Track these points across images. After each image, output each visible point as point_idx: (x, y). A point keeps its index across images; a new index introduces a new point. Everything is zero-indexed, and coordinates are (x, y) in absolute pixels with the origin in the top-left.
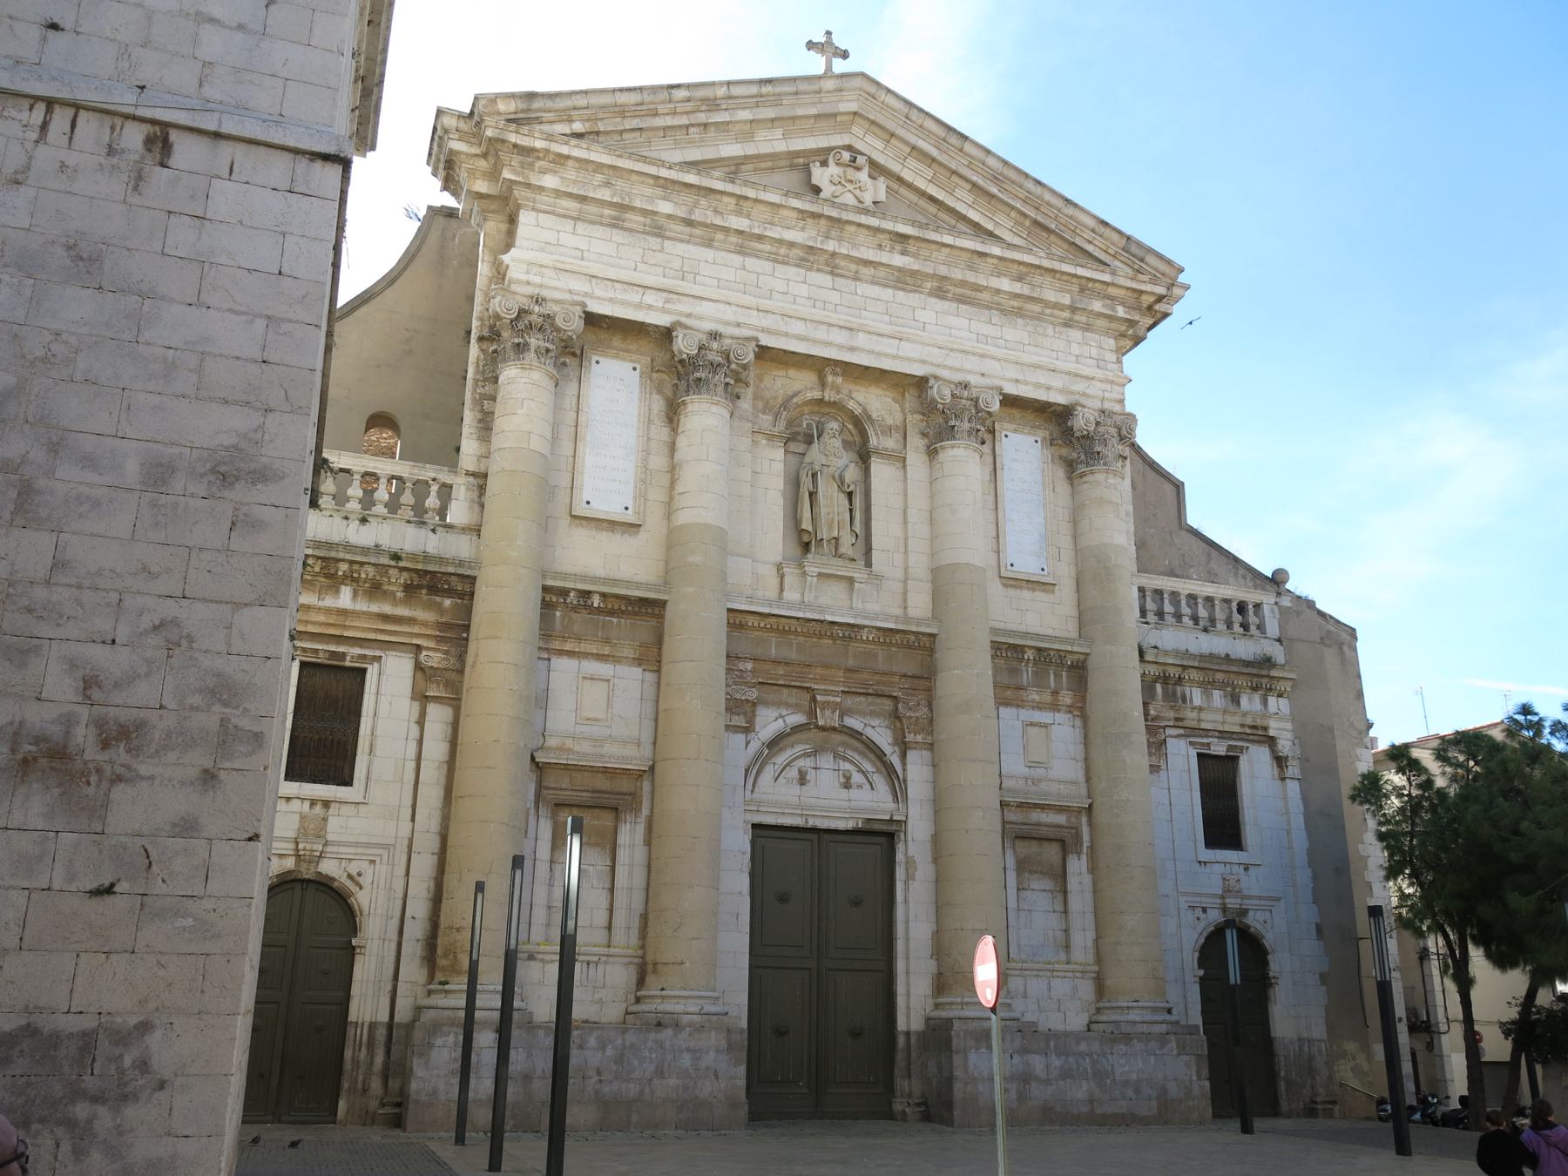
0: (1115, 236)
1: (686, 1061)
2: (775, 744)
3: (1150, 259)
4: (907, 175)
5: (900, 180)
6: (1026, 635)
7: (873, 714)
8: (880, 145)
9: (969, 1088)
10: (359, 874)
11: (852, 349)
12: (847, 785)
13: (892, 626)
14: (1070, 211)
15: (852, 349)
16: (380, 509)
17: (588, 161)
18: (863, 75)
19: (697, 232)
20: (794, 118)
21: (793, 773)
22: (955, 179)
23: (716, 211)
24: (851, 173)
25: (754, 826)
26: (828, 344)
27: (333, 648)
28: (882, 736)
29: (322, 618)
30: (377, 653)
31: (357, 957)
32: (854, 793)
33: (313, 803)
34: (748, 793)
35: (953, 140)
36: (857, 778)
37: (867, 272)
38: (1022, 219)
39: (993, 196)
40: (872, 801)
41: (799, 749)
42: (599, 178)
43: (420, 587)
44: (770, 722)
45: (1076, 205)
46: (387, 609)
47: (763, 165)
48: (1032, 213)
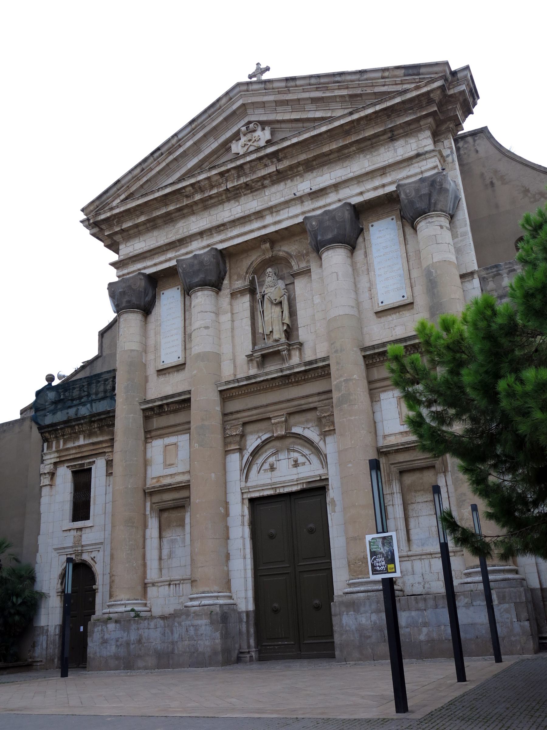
1: (192, 631)
2: (255, 453)
3: (422, 70)
4: (279, 117)
7: (307, 421)
8: (261, 111)
9: (344, 637)
10: (94, 557)
11: (264, 227)
12: (296, 464)
13: (303, 368)
14: (366, 76)
15: (264, 227)
19: (185, 211)
20: (215, 128)
21: (267, 466)
23: (187, 197)
24: (249, 136)
25: (252, 501)
26: (252, 231)
27: (80, 462)
28: (312, 434)
29: (74, 451)
30: (94, 459)
31: (97, 594)
32: (300, 469)
33: (77, 529)
34: (243, 484)
35: (291, 83)
36: (301, 460)
37: (266, 182)
40: (310, 470)
41: (269, 453)
42: (138, 213)
43: (102, 426)
44: (252, 442)
46: (95, 440)
47: (212, 159)
48: (344, 92)
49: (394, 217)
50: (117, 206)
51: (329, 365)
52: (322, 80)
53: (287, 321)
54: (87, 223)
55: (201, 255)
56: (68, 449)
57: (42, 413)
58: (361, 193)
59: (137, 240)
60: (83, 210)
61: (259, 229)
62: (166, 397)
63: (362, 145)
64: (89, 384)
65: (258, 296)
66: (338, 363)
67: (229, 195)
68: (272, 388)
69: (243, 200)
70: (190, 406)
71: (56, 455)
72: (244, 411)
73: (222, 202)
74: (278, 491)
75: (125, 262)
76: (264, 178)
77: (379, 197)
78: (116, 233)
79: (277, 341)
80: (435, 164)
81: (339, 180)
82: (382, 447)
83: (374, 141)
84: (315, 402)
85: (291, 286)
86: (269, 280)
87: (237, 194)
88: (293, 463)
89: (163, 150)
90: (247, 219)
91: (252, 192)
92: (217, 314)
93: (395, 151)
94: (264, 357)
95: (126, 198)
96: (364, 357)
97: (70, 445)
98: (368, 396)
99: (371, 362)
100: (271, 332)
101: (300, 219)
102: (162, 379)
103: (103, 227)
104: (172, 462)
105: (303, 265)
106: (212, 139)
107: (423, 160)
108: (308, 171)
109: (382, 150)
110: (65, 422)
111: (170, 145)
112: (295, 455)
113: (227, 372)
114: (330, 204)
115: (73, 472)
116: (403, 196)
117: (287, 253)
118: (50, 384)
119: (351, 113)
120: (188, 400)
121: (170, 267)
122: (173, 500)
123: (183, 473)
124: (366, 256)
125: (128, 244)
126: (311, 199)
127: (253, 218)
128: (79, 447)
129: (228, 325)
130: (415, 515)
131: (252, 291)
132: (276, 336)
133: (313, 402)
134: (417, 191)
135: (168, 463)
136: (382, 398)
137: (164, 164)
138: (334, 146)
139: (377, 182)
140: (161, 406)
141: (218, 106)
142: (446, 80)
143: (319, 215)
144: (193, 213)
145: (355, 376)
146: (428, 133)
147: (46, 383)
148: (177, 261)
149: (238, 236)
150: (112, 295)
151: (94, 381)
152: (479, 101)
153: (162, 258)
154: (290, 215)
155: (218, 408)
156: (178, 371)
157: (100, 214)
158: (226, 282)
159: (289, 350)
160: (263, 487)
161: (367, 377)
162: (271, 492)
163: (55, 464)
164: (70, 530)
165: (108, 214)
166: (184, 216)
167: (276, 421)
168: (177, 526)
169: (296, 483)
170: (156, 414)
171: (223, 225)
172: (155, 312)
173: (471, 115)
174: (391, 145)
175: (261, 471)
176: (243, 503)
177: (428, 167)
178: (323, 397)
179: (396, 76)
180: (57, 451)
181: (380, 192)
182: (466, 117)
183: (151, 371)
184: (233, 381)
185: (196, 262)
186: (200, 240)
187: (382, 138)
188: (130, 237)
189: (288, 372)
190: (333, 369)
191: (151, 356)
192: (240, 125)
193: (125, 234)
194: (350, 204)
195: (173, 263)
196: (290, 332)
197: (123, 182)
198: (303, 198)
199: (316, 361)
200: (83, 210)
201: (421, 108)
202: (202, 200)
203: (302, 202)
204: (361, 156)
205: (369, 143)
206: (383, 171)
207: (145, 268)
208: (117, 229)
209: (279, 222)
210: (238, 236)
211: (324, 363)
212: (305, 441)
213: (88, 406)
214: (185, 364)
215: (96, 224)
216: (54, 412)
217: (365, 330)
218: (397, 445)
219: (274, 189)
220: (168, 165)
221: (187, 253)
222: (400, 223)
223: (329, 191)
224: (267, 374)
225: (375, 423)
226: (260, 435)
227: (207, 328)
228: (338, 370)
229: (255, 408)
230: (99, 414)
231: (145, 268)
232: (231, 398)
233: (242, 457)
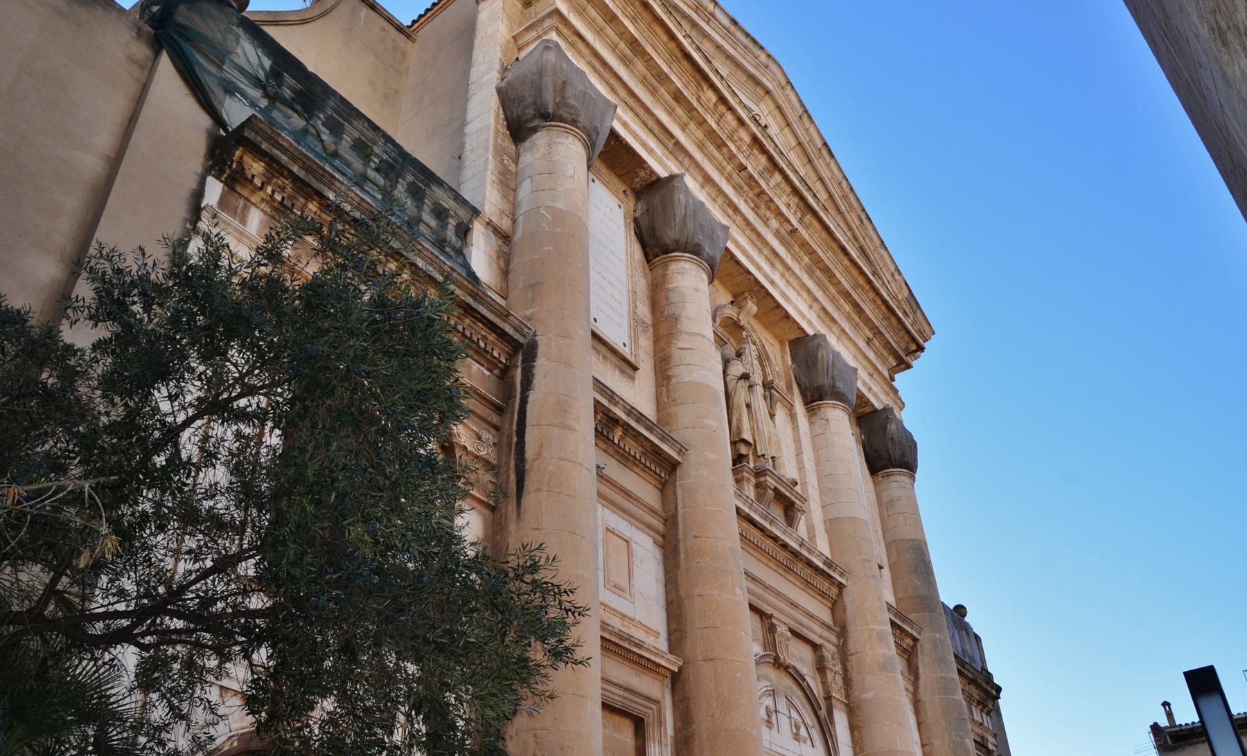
14: (883, 252)
67: (735, 176)
76: (779, 214)
87: (741, 188)
121: (645, 162)
122: (627, 689)
188: (581, 14)
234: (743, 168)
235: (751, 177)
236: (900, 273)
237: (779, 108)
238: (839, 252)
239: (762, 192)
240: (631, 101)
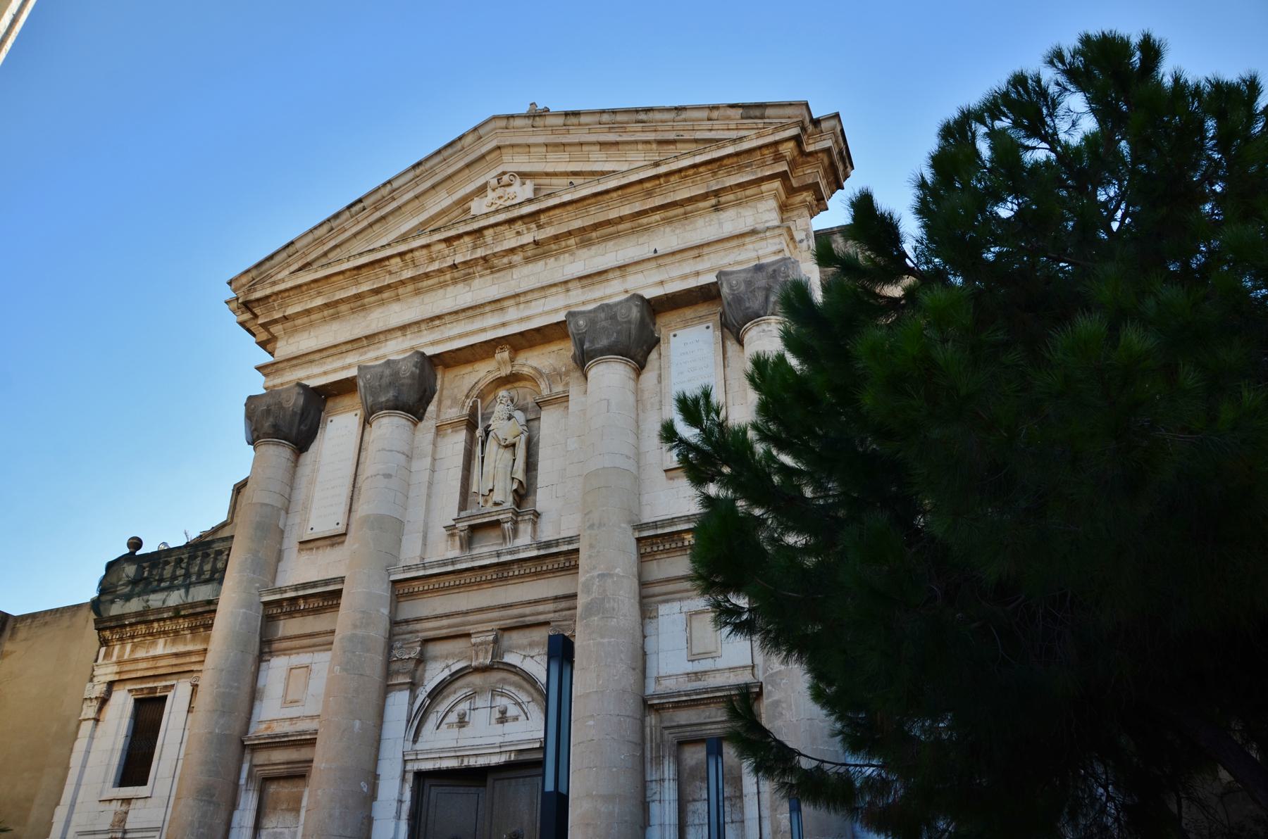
0: (731, 112)
2: (437, 693)
4: (550, 168)
5: (547, 174)
6: (672, 521)
7: (532, 645)
8: (524, 158)
11: (504, 325)
12: (503, 718)
13: (534, 553)
14: (684, 115)
15: (504, 325)
16: (194, 579)
17: (300, 286)
18: (494, 118)
19: (385, 295)
20: (449, 177)
21: (453, 718)
22: (585, 148)
23: (390, 273)
24: (500, 192)
25: (419, 775)
26: (484, 330)
33: (123, 800)
34: (409, 745)
35: (573, 120)
37: (517, 258)
38: (649, 146)
39: (617, 143)
41: (460, 694)
42: (313, 292)
43: (197, 627)
44: (435, 674)
45: (683, 109)
46: (181, 648)
49: (710, 324)
50: (283, 280)
51: (577, 550)
52: (619, 118)
53: (520, 475)
54: (234, 305)
55: (399, 361)
56: (136, 660)
57: (109, 597)
58: (662, 283)
59: (305, 335)
60: (230, 283)
61: (495, 327)
62: (305, 586)
63: (671, 213)
64: (192, 558)
65: (479, 432)
66: (591, 546)
67: (456, 275)
68: (479, 583)
69: (477, 283)
70: (338, 605)
71: (116, 669)
72: (427, 619)
73: (443, 285)
74: (466, 763)
75: (281, 366)
76: (512, 251)
77: (689, 291)
78: (275, 322)
79: (496, 504)
80: (779, 247)
81: (627, 261)
82: (653, 696)
83: (689, 208)
84: (549, 612)
85: (536, 423)
86: (500, 410)
88: (498, 715)
89: (366, 203)
90: (478, 311)
91: (492, 273)
92: (409, 457)
93: (720, 224)
94: (474, 529)
95: (300, 269)
96: (639, 540)
97: (141, 653)
98: (637, 606)
99: (649, 550)
100: (491, 491)
101: (561, 317)
102: (305, 556)
103: (257, 311)
104: (296, 698)
105: (558, 389)
106: (443, 194)
107: (762, 239)
108: (584, 246)
109: (700, 222)
110: (137, 614)
111: (378, 196)
112: (501, 702)
113: (411, 552)
114: (610, 296)
115: (136, 700)
116: (725, 290)
117: (535, 369)
118: (132, 553)
119: (657, 164)
120: (338, 594)
121: (347, 379)
122: (288, 763)
123: (312, 717)
124: (660, 382)
125: (291, 341)
126: (583, 287)
127: (488, 309)
128: (154, 658)
129: (425, 476)
130: (697, 822)
131: (471, 425)
132: (497, 497)
133: (546, 611)
134: (749, 283)
135: (289, 698)
136: (661, 612)
137: (365, 223)
138: (626, 210)
139: (688, 267)
140: (293, 600)
141: (459, 146)
142: (804, 129)
143: (590, 312)
144: (397, 298)
145: (617, 570)
146: (772, 204)
147: (127, 551)
148: (360, 368)
149: (461, 336)
150: (249, 416)
151: (200, 553)
152: (852, 173)
153: (338, 363)
154: (547, 309)
155: (385, 611)
156: (332, 545)
157: (255, 290)
158: (432, 408)
159: (516, 523)
160: (441, 753)
161: (640, 575)
162: (453, 764)
163: (111, 685)
164: (111, 801)
165: (268, 291)
166: (382, 303)
167: (478, 640)
168: (288, 810)
169: (498, 750)
170: (285, 614)
171: (439, 317)
172: (313, 448)
173: (839, 191)
174: (714, 216)
175: (443, 726)
176: (403, 780)
177: (766, 251)
178: (563, 604)
179: (729, 118)
180: (119, 663)
181: (692, 283)
182: (833, 192)
183: (291, 543)
184: (417, 567)
185: (387, 372)
186: (400, 339)
187: (701, 205)
189: (509, 558)
190: (583, 559)
191: (295, 519)
192: (490, 177)
193: (289, 324)
194: (642, 298)
195: (353, 372)
196: (523, 494)
197: (298, 245)
198: (570, 285)
199: (557, 543)
200: (230, 283)
201: (763, 165)
202: (413, 279)
203: (568, 290)
204: (668, 229)
205: (680, 211)
206: (699, 249)
207: (308, 377)
208: (277, 315)
209: (528, 318)
210: (461, 336)
211: (570, 547)
212: (524, 679)
213: (182, 591)
214: (345, 534)
215: (247, 306)
216: (127, 598)
217: (645, 498)
218: (679, 694)
219: (530, 268)
220: (371, 225)
221: (377, 359)
222: (719, 333)
223: (611, 275)
224: (473, 559)
225: (645, 654)
226: (450, 662)
227: (388, 476)
228: (590, 557)
229: (447, 616)
230: (193, 605)
231: (308, 377)
232: (412, 595)
233: (413, 698)
234: (454, 266)
235: (465, 263)
236: (715, 108)
237: (512, 146)
238: (599, 198)
239: (485, 259)
240: (325, 354)
